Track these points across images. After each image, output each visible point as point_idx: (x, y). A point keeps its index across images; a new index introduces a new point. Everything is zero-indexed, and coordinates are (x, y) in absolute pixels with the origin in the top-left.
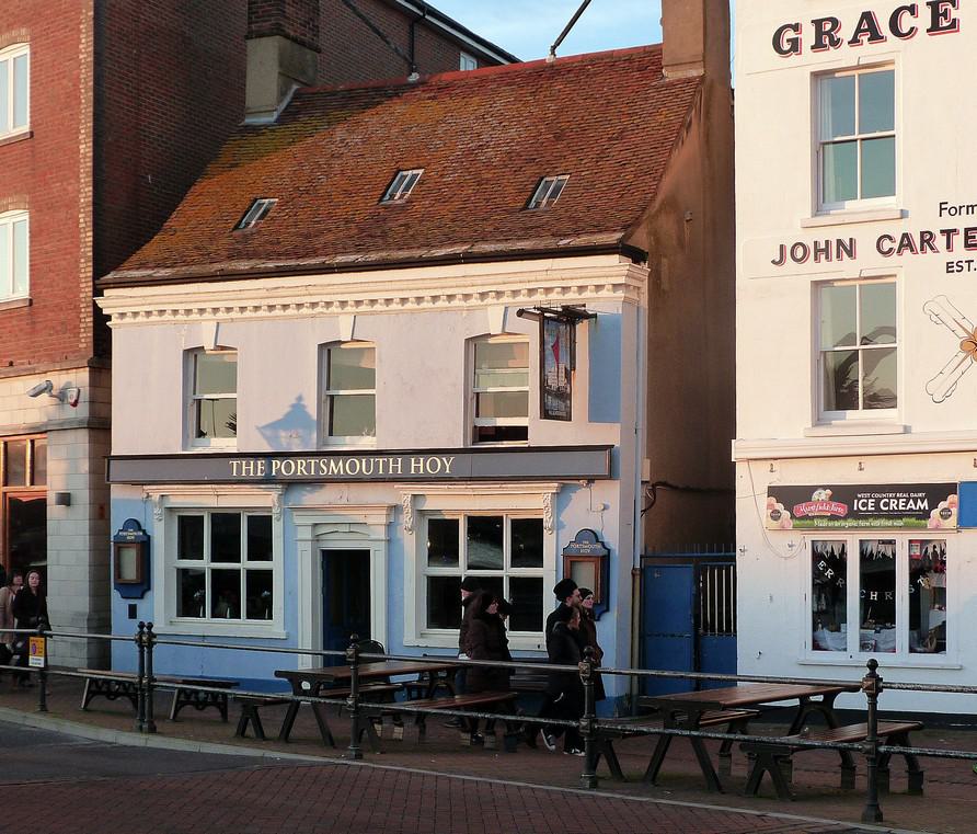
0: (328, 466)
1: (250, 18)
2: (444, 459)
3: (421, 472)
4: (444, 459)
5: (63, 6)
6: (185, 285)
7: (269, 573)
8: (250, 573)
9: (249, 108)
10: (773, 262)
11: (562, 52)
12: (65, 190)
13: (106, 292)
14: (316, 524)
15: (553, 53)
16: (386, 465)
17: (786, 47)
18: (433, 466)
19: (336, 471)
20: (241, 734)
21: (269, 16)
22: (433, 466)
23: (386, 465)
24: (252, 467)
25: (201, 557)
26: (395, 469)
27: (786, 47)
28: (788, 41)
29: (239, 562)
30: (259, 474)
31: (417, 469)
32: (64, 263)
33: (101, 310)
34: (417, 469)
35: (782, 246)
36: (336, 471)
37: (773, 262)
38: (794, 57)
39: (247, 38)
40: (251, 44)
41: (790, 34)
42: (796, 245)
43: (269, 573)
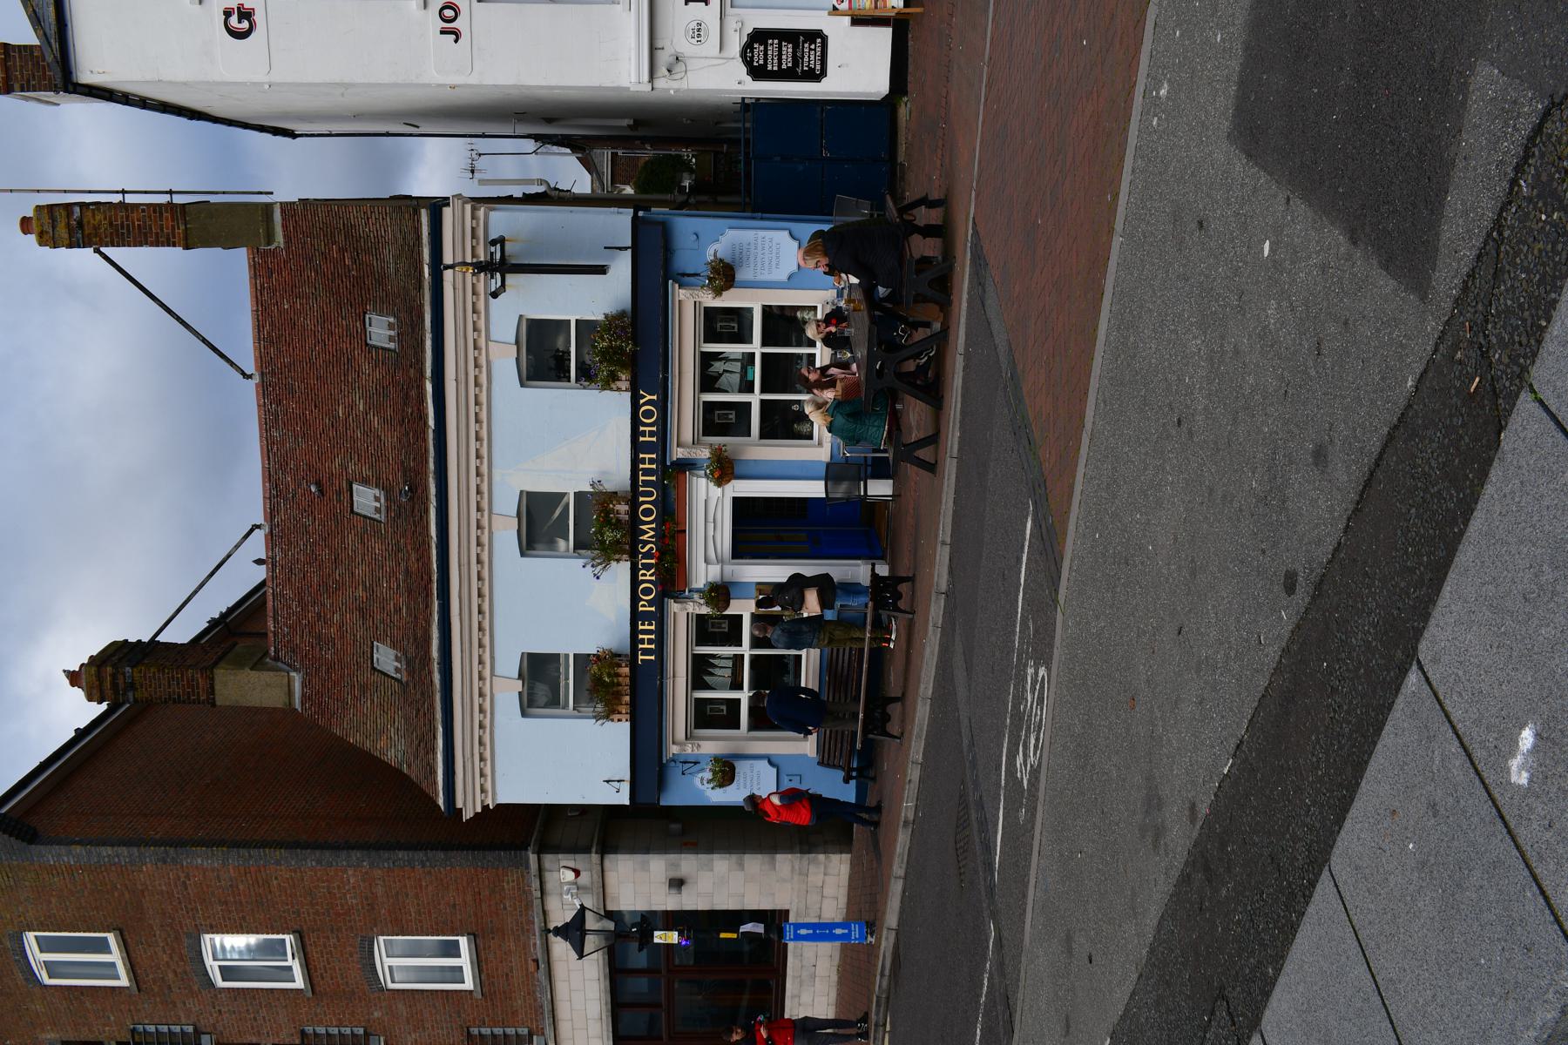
0: (645, 543)
1: (194, 702)
2: (642, 401)
3: (654, 429)
4: (642, 401)
5: (164, 888)
6: (454, 705)
7: (767, 311)
8: (764, 343)
9: (285, 704)
10: (456, 41)
11: (250, 367)
12: (354, 888)
13: (459, 805)
14: (705, 561)
15: (249, 377)
16: (647, 472)
17: (245, 25)
18: (648, 414)
19: (652, 533)
20: (931, 467)
21: (193, 680)
22: (648, 414)
23: (647, 472)
24: (646, 637)
25: (749, 404)
26: (651, 461)
27: (245, 25)
28: (240, 22)
29: (743, 656)
30: (653, 627)
31: (651, 434)
32: (430, 888)
33: (476, 814)
34: (651, 434)
35: (442, 32)
36: (652, 533)
37: (456, 41)
38: (258, 17)
39: (214, 705)
40: (218, 703)
41: (234, 21)
42: (440, 14)
43: (767, 311)
